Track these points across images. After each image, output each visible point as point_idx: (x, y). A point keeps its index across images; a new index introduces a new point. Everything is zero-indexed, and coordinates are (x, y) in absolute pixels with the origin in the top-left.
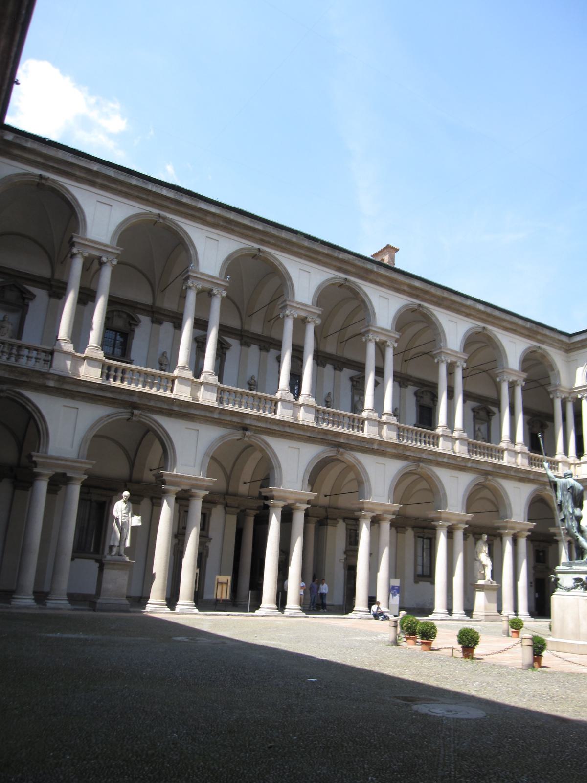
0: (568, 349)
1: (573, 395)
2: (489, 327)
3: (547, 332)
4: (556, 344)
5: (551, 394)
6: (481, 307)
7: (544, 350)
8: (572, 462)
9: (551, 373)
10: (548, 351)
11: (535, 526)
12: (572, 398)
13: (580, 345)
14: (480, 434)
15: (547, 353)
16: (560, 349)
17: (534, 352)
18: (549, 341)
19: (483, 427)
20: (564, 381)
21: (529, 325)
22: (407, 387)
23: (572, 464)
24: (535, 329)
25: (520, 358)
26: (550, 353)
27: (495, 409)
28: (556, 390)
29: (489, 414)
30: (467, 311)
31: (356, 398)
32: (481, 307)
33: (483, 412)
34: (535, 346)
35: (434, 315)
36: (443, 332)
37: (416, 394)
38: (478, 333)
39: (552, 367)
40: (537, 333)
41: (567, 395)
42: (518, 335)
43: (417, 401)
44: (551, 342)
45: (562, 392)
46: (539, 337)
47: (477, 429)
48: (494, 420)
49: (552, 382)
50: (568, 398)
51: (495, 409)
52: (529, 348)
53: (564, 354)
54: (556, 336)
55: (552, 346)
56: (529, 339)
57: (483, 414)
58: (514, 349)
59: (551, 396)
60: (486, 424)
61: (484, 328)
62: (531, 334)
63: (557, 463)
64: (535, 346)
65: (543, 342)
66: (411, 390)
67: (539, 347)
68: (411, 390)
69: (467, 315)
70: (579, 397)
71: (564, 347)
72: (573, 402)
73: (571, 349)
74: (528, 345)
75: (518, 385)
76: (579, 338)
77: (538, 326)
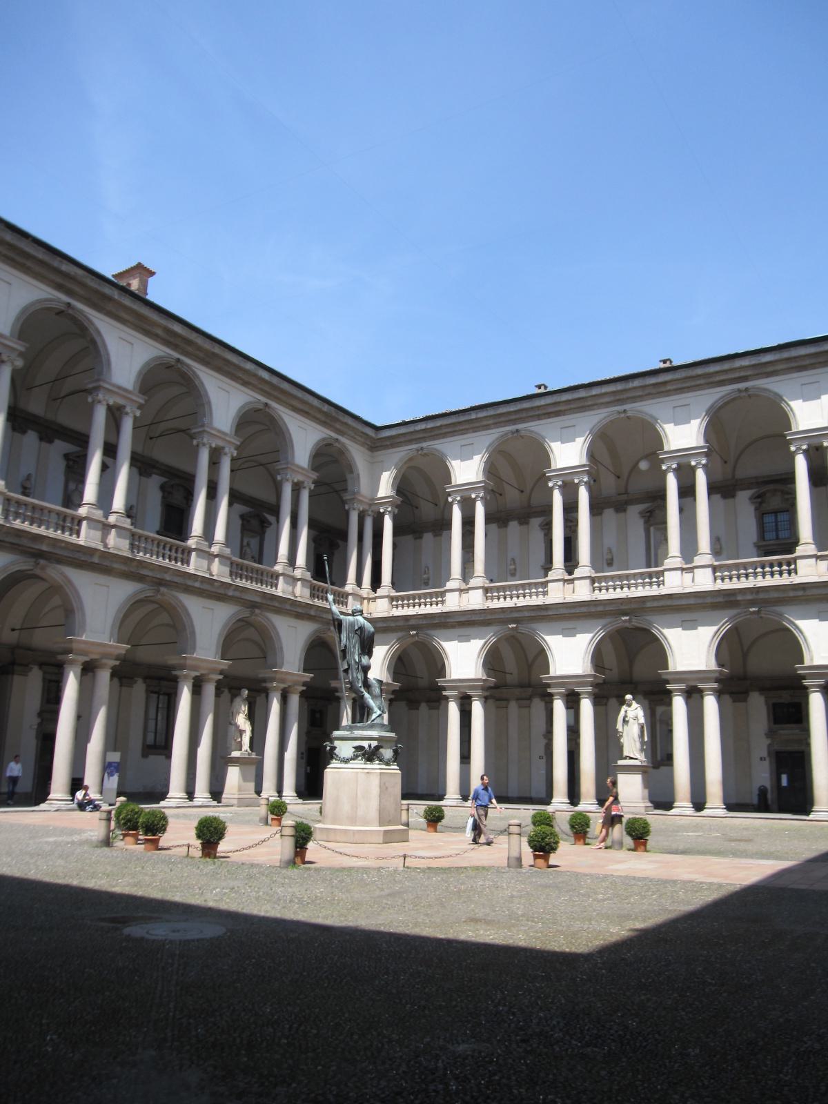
0: (373, 446)
1: (374, 508)
4: (359, 438)
7: (343, 444)
8: (365, 596)
9: (349, 476)
11: (312, 678)
12: (372, 511)
16: (363, 444)
18: (350, 432)
19: (254, 542)
20: (364, 487)
21: (326, 408)
23: (364, 599)
24: (334, 414)
25: (311, 451)
27: (271, 518)
29: (264, 524)
33: (255, 521)
34: (331, 438)
39: (351, 468)
40: (337, 420)
41: (367, 507)
44: (353, 435)
45: (361, 502)
46: (338, 426)
47: (245, 543)
48: (269, 533)
49: (350, 488)
50: (367, 511)
51: (271, 518)
52: (324, 439)
53: (367, 451)
55: (353, 439)
56: (325, 427)
57: (255, 523)
62: (328, 421)
63: (347, 595)
67: (337, 439)
71: (369, 443)
72: (373, 516)
73: (377, 447)
75: (304, 488)
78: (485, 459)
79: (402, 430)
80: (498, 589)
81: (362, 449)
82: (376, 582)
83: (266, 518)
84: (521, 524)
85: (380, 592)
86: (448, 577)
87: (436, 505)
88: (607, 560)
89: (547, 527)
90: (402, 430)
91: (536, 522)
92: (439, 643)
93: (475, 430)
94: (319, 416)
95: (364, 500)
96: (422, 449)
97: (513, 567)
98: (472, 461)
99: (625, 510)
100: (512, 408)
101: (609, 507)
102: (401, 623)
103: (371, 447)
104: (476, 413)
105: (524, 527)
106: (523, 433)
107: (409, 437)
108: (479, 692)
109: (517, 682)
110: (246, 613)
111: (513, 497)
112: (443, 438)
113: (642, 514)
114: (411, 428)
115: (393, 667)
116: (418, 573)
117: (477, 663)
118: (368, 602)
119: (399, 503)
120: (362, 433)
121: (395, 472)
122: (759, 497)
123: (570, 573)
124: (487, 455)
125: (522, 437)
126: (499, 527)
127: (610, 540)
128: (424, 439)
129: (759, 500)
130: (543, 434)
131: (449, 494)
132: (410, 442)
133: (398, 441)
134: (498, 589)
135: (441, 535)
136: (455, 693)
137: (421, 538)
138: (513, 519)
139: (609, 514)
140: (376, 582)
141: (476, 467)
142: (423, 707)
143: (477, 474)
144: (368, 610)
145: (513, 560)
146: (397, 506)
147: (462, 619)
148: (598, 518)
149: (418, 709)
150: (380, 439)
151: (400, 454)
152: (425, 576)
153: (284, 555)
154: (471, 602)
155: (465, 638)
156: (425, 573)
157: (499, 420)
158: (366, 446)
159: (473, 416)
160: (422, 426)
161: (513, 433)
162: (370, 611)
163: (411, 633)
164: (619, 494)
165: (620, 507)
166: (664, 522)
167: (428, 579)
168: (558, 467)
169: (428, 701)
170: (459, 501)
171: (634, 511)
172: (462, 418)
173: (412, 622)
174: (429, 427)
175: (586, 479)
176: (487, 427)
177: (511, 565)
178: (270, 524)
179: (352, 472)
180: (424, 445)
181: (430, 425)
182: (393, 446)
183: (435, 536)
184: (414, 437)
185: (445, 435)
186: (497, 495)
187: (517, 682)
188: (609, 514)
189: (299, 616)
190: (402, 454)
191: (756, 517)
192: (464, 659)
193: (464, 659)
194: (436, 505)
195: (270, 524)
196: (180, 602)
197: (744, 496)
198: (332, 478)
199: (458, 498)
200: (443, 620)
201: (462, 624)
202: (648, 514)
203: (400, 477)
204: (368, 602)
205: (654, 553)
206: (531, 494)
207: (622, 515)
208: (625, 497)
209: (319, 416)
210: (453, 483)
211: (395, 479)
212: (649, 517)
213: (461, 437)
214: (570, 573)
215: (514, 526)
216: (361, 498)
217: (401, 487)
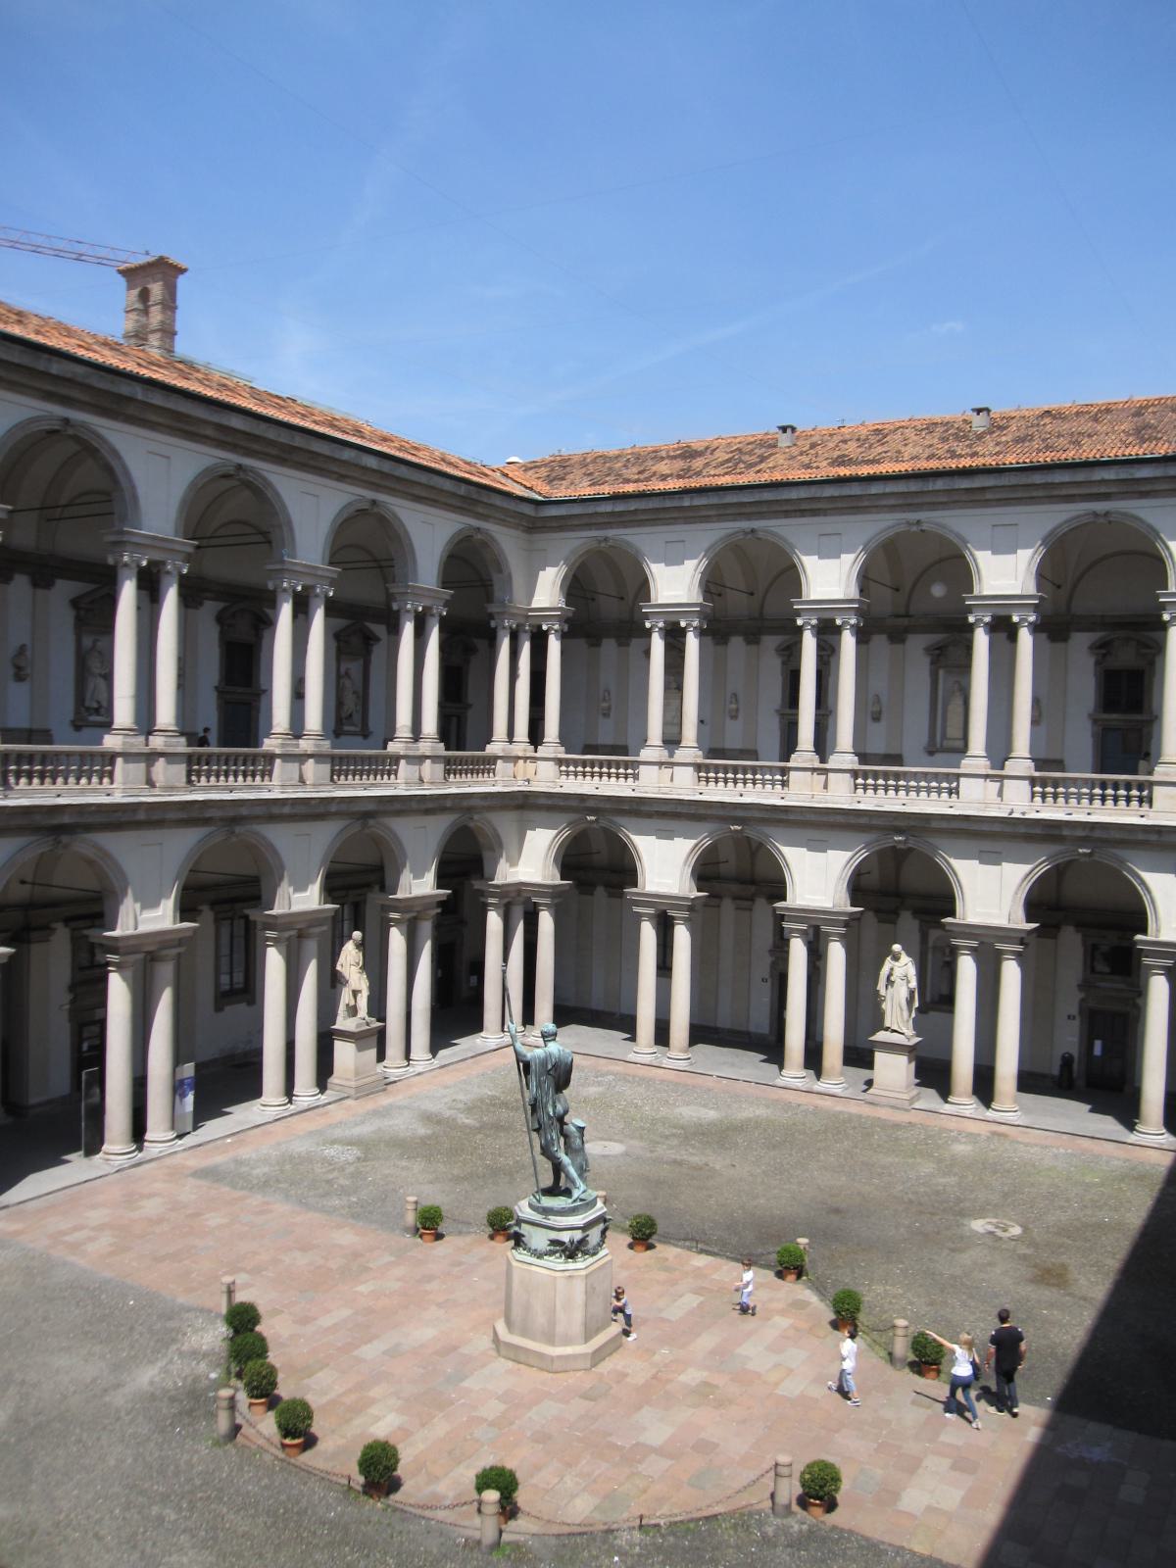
2: (382, 497)
3: (498, 501)
4: (509, 519)
5: (493, 619)
6: (372, 462)
7: (486, 533)
8: (520, 754)
9: (495, 577)
10: (494, 534)
12: (529, 626)
13: (554, 524)
14: (347, 683)
15: (493, 538)
16: (516, 527)
17: (468, 538)
19: (354, 667)
20: (520, 603)
21: (463, 490)
22: (201, 604)
23: (520, 758)
24: (475, 496)
25: (441, 557)
26: (497, 536)
27: (379, 630)
28: (503, 613)
29: (369, 639)
30: (343, 471)
31: (87, 642)
32: (372, 462)
33: (360, 638)
35: (269, 484)
36: (290, 523)
37: (220, 619)
38: (362, 512)
39: (499, 565)
40: (477, 502)
42: (440, 508)
43: (222, 633)
45: (513, 616)
47: (343, 670)
48: (378, 653)
49: (497, 594)
51: (379, 630)
53: (524, 536)
54: (512, 506)
55: (502, 522)
58: (429, 536)
60: (361, 662)
61: (374, 502)
62: (465, 506)
66: (210, 608)
67: (479, 529)
68: (210, 608)
69: (341, 478)
72: (531, 632)
74: (458, 527)
76: (553, 511)
77: (480, 490)
78: (702, 568)
79: (577, 510)
80: (717, 769)
81: (513, 532)
82: (536, 736)
83: (371, 632)
84: (749, 642)
85: (542, 751)
86: (643, 741)
87: (622, 598)
88: (873, 713)
89: (786, 653)
90: (577, 510)
91: (771, 642)
92: (628, 837)
93: (688, 520)
94: (453, 501)
96: (606, 539)
97: (734, 706)
98: (681, 566)
102: (574, 803)
103: (529, 528)
104: (692, 498)
106: (761, 535)
108: (686, 914)
109: (739, 872)
110: (357, 827)
111: (738, 604)
112: (639, 526)
113: (928, 650)
114: (591, 509)
116: (603, 733)
117: (682, 874)
118: (525, 762)
119: (570, 615)
120: (515, 512)
121: (564, 569)
123: (823, 760)
124: (705, 562)
125: (759, 539)
126: (717, 644)
127: (879, 684)
129: (1104, 651)
131: (647, 616)
132: (589, 526)
133: (570, 523)
134: (717, 769)
135: (628, 645)
136: (651, 911)
137: (598, 644)
138: (737, 633)
139: (879, 641)
140: (536, 736)
141: (688, 580)
142: (600, 891)
143: (689, 590)
144: (525, 773)
145: (735, 695)
146: (567, 621)
147: (664, 809)
149: (592, 894)
150: (538, 519)
151: (575, 542)
152: (605, 705)
153: (404, 726)
155: (668, 835)
156: (604, 700)
157: (724, 513)
158: (521, 528)
159: (686, 502)
160: (607, 508)
161: (746, 533)
162: (528, 777)
164: (898, 616)
165: (897, 636)
166: (965, 666)
167: (609, 708)
168: (812, 598)
169: (608, 885)
170: (660, 629)
172: (668, 504)
173: (590, 804)
174: (617, 510)
175: (853, 621)
176: (706, 519)
177: (731, 703)
178: (378, 639)
179: (500, 571)
180: (611, 533)
181: (620, 507)
182: (561, 529)
183: (620, 645)
184: (594, 521)
185: (641, 523)
186: (716, 597)
187: (739, 872)
189: (428, 812)
191: (1095, 675)
192: (665, 866)
193: (665, 866)
194: (622, 598)
195: (378, 639)
196: (264, 838)
198: (473, 576)
199: (661, 625)
200: (635, 807)
201: (663, 815)
202: (937, 652)
203: (571, 577)
204: (525, 762)
205: (947, 745)
206: (764, 597)
208: (905, 621)
209: (453, 501)
212: (939, 655)
214: (823, 760)
215: (737, 643)
216: (515, 611)
217: (576, 588)
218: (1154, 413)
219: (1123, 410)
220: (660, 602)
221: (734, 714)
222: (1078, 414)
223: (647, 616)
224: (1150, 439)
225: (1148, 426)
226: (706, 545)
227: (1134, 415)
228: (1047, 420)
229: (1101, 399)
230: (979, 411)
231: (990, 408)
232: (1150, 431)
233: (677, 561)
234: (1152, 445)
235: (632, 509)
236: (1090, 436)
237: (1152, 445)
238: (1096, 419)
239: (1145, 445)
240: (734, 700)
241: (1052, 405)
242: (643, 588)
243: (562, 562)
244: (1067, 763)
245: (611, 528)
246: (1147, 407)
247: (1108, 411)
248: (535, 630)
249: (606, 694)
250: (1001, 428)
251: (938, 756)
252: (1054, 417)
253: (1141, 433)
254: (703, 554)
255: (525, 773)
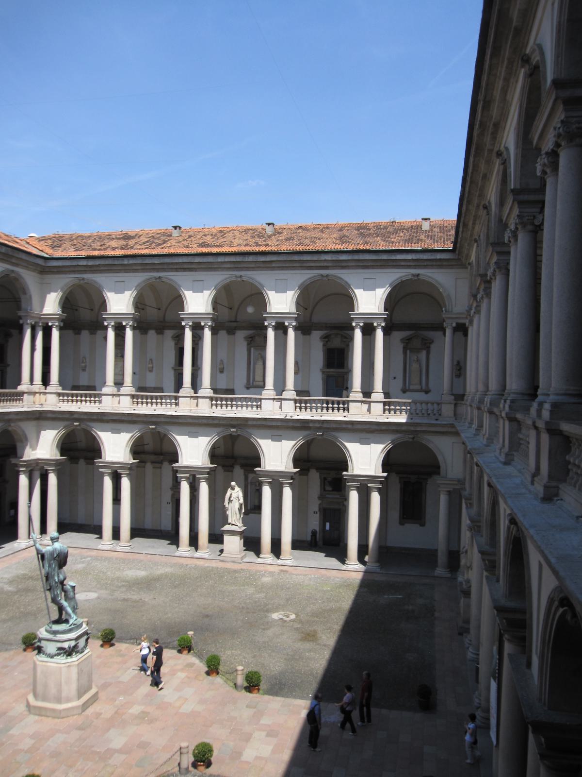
0: (42, 270)
3: (24, 256)
5: (21, 319)
7: (17, 273)
8: (37, 391)
9: (23, 297)
10: (21, 274)
12: (42, 323)
16: (34, 271)
20: (36, 310)
24: (11, 254)
28: (27, 316)
34: (8, 270)
39: (25, 291)
40: (13, 257)
41: (37, 320)
45: (33, 318)
46: (14, 261)
49: (23, 305)
50: (39, 323)
55: (26, 268)
59: (21, 322)
63: (22, 394)
64: (8, 269)
65: (17, 265)
70: (50, 324)
71: (38, 269)
72: (43, 326)
78: (134, 295)
79: (68, 263)
80: (142, 397)
82: (46, 381)
85: (49, 389)
86: (104, 383)
87: (92, 310)
88: (220, 369)
89: (177, 339)
90: (68, 263)
91: (169, 333)
92: (96, 432)
93: (126, 271)
95: (35, 315)
96: (83, 279)
97: (150, 365)
99: (234, 334)
100: (156, 261)
101: (223, 329)
102: (67, 416)
103: (41, 271)
104: (128, 260)
105: (160, 336)
106: (164, 280)
107: (72, 269)
108: (127, 472)
109: (154, 450)
111: (152, 314)
112: (101, 273)
113: (246, 338)
114: (75, 263)
115: (60, 445)
116: (81, 378)
117: (125, 451)
118: (40, 395)
119: (64, 318)
120: (33, 262)
121: (61, 294)
122: (325, 338)
123: (196, 392)
124: (135, 293)
127: (223, 354)
128: (85, 272)
129: (327, 340)
130: (180, 283)
131: (105, 319)
132: (74, 272)
134: (142, 397)
135: (95, 334)
136: (109, 471)
137: (79, 334)
138: (151, 329)
139: (223, 334)
140: (46, 381)
142: (82, 462)
143: (127, 307)
144: (40, 401)
145: (151, 360)
146: (63, 321)
147: (115, 418)
148: (215, 336)
149: (77, 463)
150: (46, 267)
151: (67, 280)
152: (83, 365)
154: (121, 404)
155: (117, 431)
156: (83, 362)
157: (145, 268)
159: (126, 262)
160: (84, 263)
161: (156, 279)
163: (75, 424)
164: (231, 322)
165: (231, 331)
166: (263, 346)
167: (85, 366)
168: (190, 312)
169: (86, 459)
170: (112, 326)
171: (241, 335)
172: (116, 262)
173: (76, 416)
175: (210, 324)
176: (136, 271)
177: (149, 364)
179: (25, 293)
180: (85, 276)
181: (91, 263)
183: (91, 333)
184: (76, 269)
185: (102, 271)
187: (154, 450)
188: (223, 334)
190: (68, 280)
191: (323, 351)
192: (116, 447)
193: (116, 447)
197: (317, 335)
202: (251, 339)
204: (40, 395)
205: (255, 384)
206: (166, 311)
207: (232, 336)
208: (234, 324)
210: (108, 312)
211: (61, 299)
213: (115, 275)
214: (196, 392)
215: (152, 334)
216: (32, 315)
217: (67, 303)
218: (347, 230)
219: (334, 228)
220: (112, 312)
221: (151, 369)
222: (314, 228)
223: (105, 319)
224: (346, 242)
225: (345, 236)
226: (136, 284)
227: (339, 231)
228: (300, 231)
229: (324, 222)
230: (269, 224)
231: (274, 223)
232: (346, 238)
233: (121, 291)
234: (347, 245)
235: (97, 264)
236: (319, 239)
237: (347, 245)
238: (322, 231)
239: (344, 245)
240: (150, 362)
241: (303, 224)
242: (103, 305)
243: (59, 290)
244: (311, 393)
245: (86, 273)
246: (344, 227)
247: (327, 228)
248: (45, 325)
249: (84, 359)
250: (279, 233)
251: (252, 390)
252: (303, 229)
253: (342, 239)
254: (134, 288)
255: (40, 401)
